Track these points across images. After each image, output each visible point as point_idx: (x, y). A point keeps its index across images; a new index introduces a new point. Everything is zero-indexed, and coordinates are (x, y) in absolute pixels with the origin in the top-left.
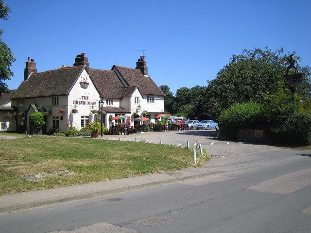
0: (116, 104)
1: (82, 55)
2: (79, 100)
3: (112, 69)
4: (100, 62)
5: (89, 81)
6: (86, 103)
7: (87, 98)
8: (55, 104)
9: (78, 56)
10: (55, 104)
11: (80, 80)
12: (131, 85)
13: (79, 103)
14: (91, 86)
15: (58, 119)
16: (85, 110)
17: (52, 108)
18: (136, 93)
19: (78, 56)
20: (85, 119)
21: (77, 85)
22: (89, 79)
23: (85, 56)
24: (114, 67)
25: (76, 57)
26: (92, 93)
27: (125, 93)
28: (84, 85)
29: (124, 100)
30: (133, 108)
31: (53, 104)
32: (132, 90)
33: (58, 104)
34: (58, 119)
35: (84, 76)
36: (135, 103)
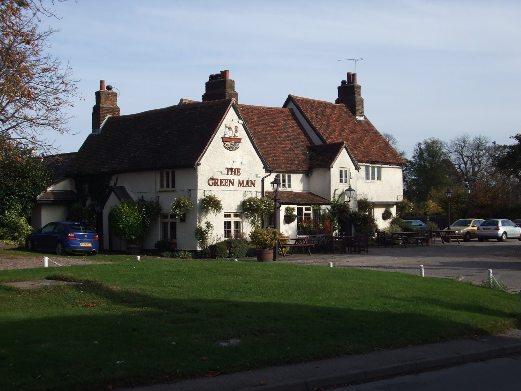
0: (297, 184)
1: (224, 74)
2: (219, 177)
3: (285, 106)
4: (259, 89)
5: (242, 134)
6: (236, 183)
7: (235, 171)
8: (168, 186)
9: (212, 77)
10: (168, 186)
11: (221, 131)
12: (329, 141)
13: (221, 182)
14: (246, 144)
15: (173, 220)
16: (231, 199)
17: (159, 194)
18: (343, 160)
19: (212, 77)
20: (233, 219)
21: (216, 143)
22: (241, 129)
23: (231, 76)
24: (290, 99)
25: (207, 80)
26: (247, 159)
27: (319, 158)
28: (231, 143)
29: (316, 176)
30: (337, 188)
31: (162, 187)
32: (332, 152)
33: (174, 186)
34: (173, 220)
35: (231, 118)
36: (341, 181)
